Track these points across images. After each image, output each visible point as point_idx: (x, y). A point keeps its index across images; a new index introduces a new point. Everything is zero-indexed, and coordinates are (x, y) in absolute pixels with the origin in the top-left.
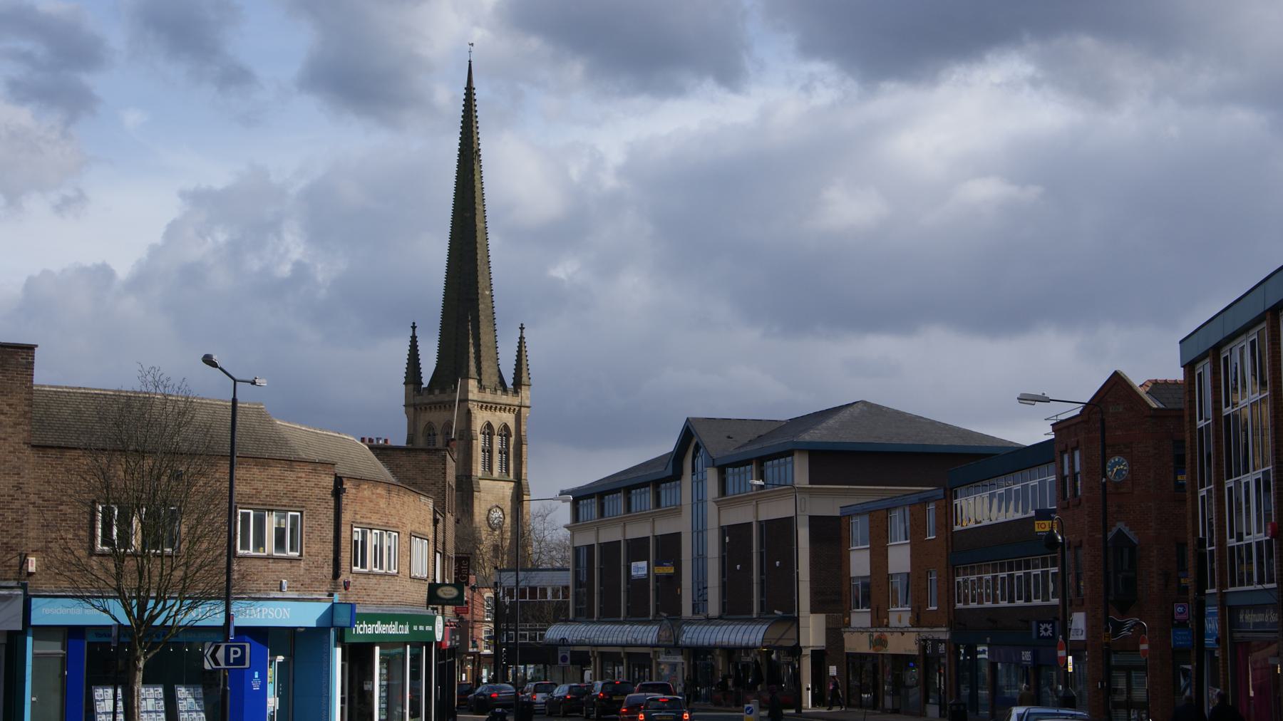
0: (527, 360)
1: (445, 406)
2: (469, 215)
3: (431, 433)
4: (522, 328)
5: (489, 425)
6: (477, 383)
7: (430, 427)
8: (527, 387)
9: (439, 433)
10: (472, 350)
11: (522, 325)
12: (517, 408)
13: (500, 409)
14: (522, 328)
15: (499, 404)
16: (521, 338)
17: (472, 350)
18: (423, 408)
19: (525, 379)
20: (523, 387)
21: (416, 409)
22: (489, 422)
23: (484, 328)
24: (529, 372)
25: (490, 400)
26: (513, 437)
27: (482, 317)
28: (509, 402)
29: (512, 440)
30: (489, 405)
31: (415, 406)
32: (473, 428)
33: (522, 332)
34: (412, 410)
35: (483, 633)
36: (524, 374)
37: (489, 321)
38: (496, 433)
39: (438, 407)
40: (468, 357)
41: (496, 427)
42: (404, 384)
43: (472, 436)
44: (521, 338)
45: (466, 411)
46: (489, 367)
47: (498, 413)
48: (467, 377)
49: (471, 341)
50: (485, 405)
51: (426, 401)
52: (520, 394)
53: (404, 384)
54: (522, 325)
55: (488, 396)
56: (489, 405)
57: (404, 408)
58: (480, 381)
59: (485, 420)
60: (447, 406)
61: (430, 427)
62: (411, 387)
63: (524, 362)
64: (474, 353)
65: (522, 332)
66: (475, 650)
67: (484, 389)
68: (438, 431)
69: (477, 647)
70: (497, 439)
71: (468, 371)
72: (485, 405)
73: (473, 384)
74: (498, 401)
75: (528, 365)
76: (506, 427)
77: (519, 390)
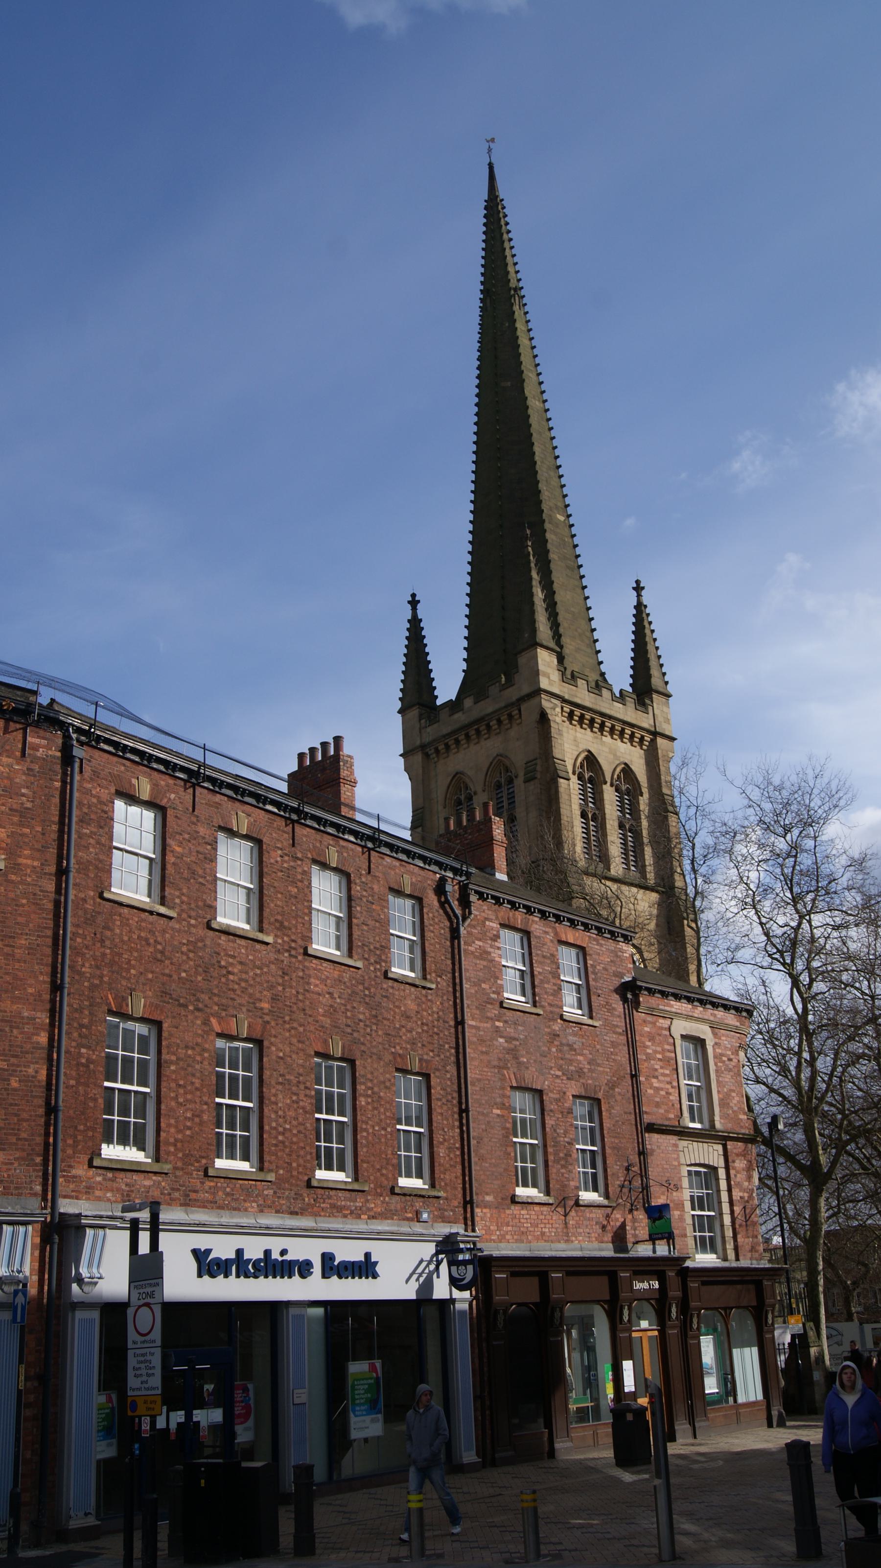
0: (657, 648)
1: (489, 727)
2: (509, 384)
3: (462, 797)
4: (638, 588)
5: (591, 760)
6: (555, 661)
7: (458, 781)
8: (662, 699)
9: (479, 789)
10: (539, 594)
11: (638, 582)
12: (648, 738)
13: (612, 731)
14: (638, 588)
15: (610, 717)
16: (640, 608)
17: (539, 594)
18: (441, 747)
19: (656, 682)
20: (655, 696)
21: (427, 756)
22: (589, 751)
23: (559, 577)
24: (666, 679)
25: (587, 704)
26: (646, 795)
27: (552, 556)
28: (628, 719)
29: (644, 802)
30: (588, 716)
31: (423, 747)
32: (557, 753)
33: (639, 596)
34: (418, 758)
35: (685, 1182)
36: (655, 672)
37: (568, 567)
38: (608, 779)
39: (472, 732)
40: (532, 604)
41: (607, 766)
42: (399, 712)
43: (556, 769)
44: (640, 608)
45: (536, 716)
46: (578, 650)
47: (607, 739)
48: (534, 644)
49: (534, 574)
50: (578, 712)
51: (445, 730)
52: (650, 708)
53: (399, 712)
54: (638, 582)
55: (582, 695)
56: (588, 716)
57: (402, 760)
58: (561, 659)
59: (583, 746)
60: (493, 723)
61: (458, 781)
62: (414, 713)
63: (650, 648)
64: (544, 601)
65: (639, 596)
66: (662, 1250)
67: (573, 677)
68: (477, 783)
69: (669, 1237)
70: (610, 795)
71: (534, 631)
72: (578, 712)
73: (546, 660)
74: (608, 712)
75: (657, 648)
76: (627, 771)
77: (648, 701)
